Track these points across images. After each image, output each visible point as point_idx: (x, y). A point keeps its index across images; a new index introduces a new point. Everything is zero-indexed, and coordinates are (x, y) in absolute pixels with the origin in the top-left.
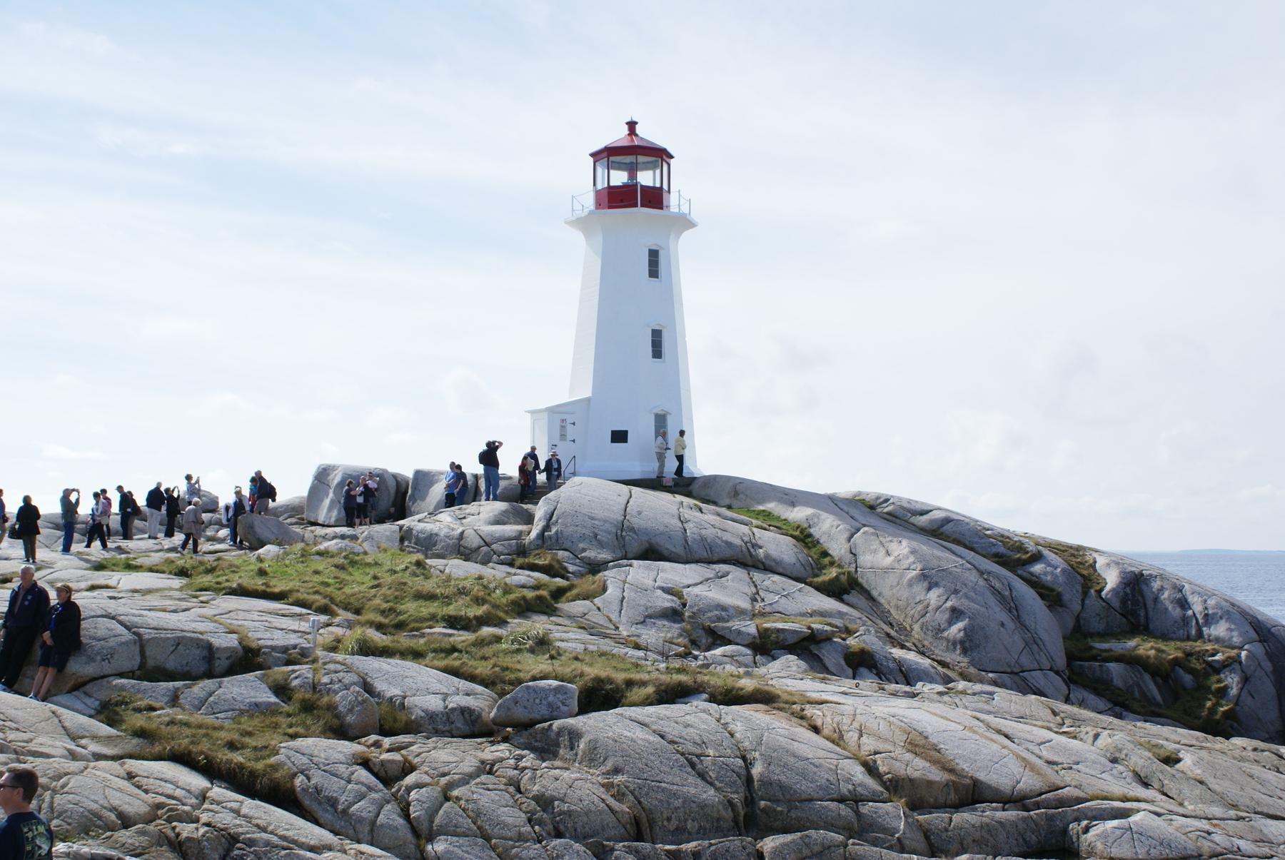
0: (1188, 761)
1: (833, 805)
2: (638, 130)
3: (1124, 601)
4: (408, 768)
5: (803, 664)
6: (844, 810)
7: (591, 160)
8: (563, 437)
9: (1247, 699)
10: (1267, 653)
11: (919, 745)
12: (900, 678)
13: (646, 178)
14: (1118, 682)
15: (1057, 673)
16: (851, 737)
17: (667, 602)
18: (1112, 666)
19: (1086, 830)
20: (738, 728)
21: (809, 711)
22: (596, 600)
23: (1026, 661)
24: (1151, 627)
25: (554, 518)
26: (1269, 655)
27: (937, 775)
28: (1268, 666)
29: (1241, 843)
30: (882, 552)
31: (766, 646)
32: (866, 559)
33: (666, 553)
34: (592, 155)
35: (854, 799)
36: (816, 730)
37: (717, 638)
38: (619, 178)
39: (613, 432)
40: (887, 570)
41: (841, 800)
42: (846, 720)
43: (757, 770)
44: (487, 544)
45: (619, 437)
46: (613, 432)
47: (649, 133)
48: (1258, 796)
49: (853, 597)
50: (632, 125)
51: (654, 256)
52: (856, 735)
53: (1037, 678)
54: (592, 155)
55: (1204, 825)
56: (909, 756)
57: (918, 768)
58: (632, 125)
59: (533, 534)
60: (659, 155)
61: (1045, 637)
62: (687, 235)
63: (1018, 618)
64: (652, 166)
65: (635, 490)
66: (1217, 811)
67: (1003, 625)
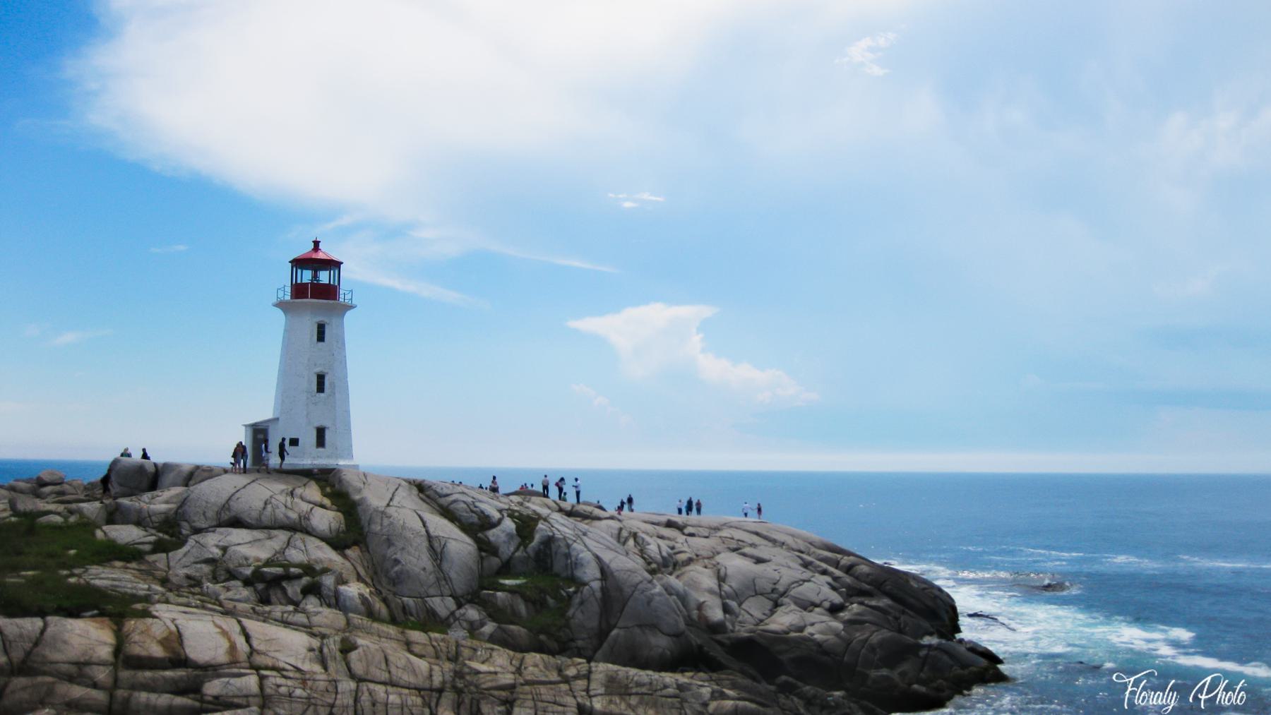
1: (66, 666)
3: (538, 553)
6: (73, 669)
9: (579, 615)
12: (333, 601)
13: (324, 277)
14: (499, 603)
15: (454, 598)
17: (217, 552)
18: (499, 594)
22: (170, 554)
23: (432, 591)
26: (602, 589)
28: (599, 595)
37: (232, 575)
38: (307, 276)
47: (327, 251)
49: (353, 553)
50: (316, 243)
58: (316, 243)
60: (333, 265)
61: (453, 575)
62: (349, 315)
63: (439, 566)
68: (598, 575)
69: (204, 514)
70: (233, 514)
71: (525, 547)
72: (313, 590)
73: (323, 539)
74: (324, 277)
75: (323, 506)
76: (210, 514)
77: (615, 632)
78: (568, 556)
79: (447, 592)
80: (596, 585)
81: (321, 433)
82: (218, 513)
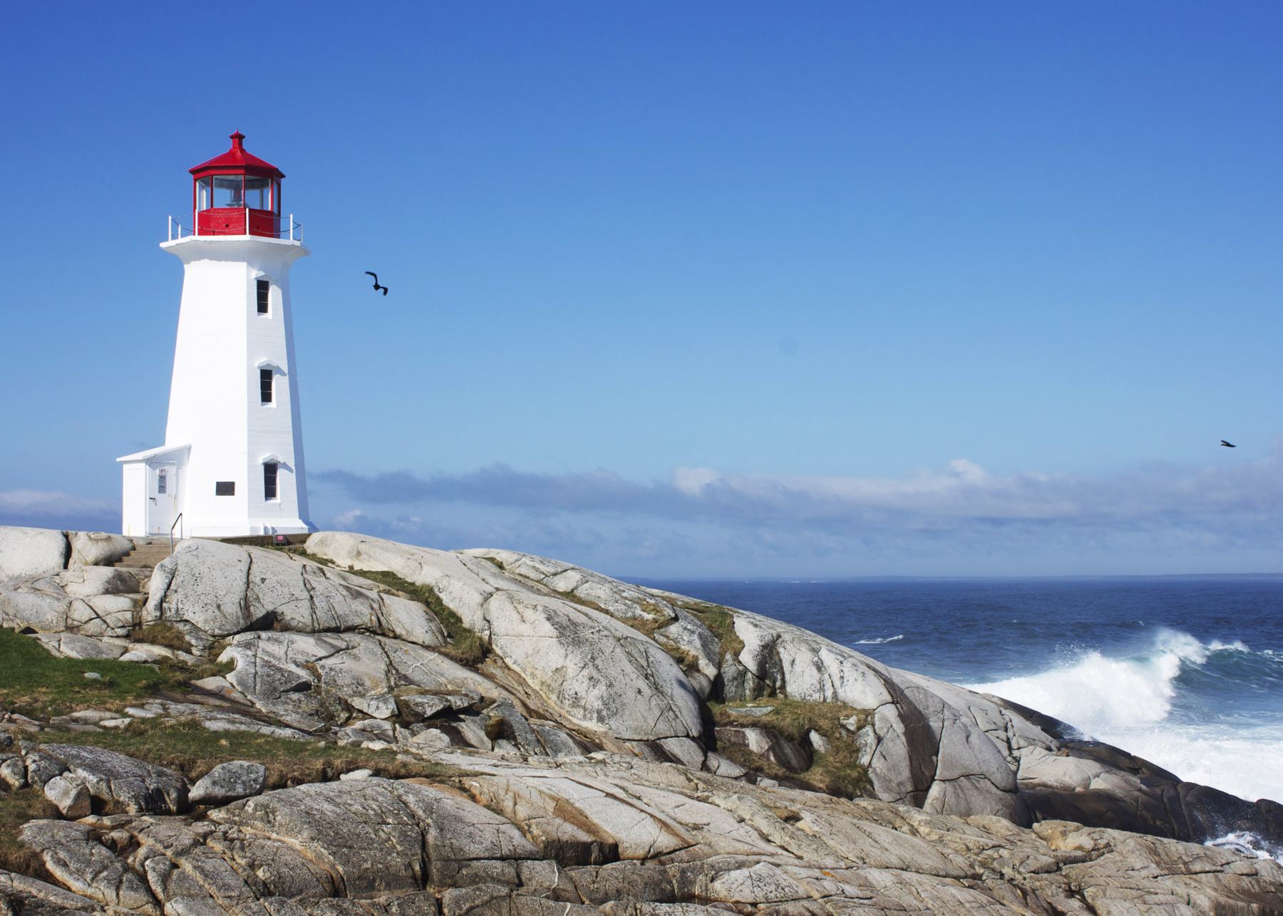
0: (807, 823)
1: (498, 864)
2: (249, 146)
4: (134, 844)
5: (446, 738)
6: (509, 871)
7: (191, 176)
8: (162, 489)
10: (900, 715)
11: (565, 810)
16: (508, 805)
19: (712, 880)
20: (411, 799)
21: (468, 782)
23: (662, 728)
24: (789, 689)
25: (173, 587)
26: (902, 717)
27: (584, 837)
29: (847, 888)
30: (515, 616)
31: (405, 717)
32: (500, 626)
33: (294, 623)
34: (193, 172)
35: (515, 858)
36: (473, 798)
39: (219, 484)
40: (519, 636)
41: (502, 859)
42: (502, 792)
43: (432, 836)
44: (98, 616)
45: (225, 489)
46: (219, 484)
48: (867, 848)
50: (238, 138)
51: (262, 287)
52: (511, 804)
53: (672, 746)
54: (193, 172)
55: (817, 873)
56: (558, 821)
57: (568, 831)
58: (238, 138)
59: (152, 603)
64: (261, 185)
65: (256, 552)
66: (829, 861)
67: (640, 692)
68: (889, 698)
69: (219, 607)
70: (270, 608)
71: (736, 654)
72: (500, 732)
73: (427, 647)
74: (252, 199)
75: (388, 592)
76: (232, 607)
77: (935, 790)
78: (819, 667)
79: (681, 731)
80: (891, 712)
81: (270, 470)
82: (246, 605)
